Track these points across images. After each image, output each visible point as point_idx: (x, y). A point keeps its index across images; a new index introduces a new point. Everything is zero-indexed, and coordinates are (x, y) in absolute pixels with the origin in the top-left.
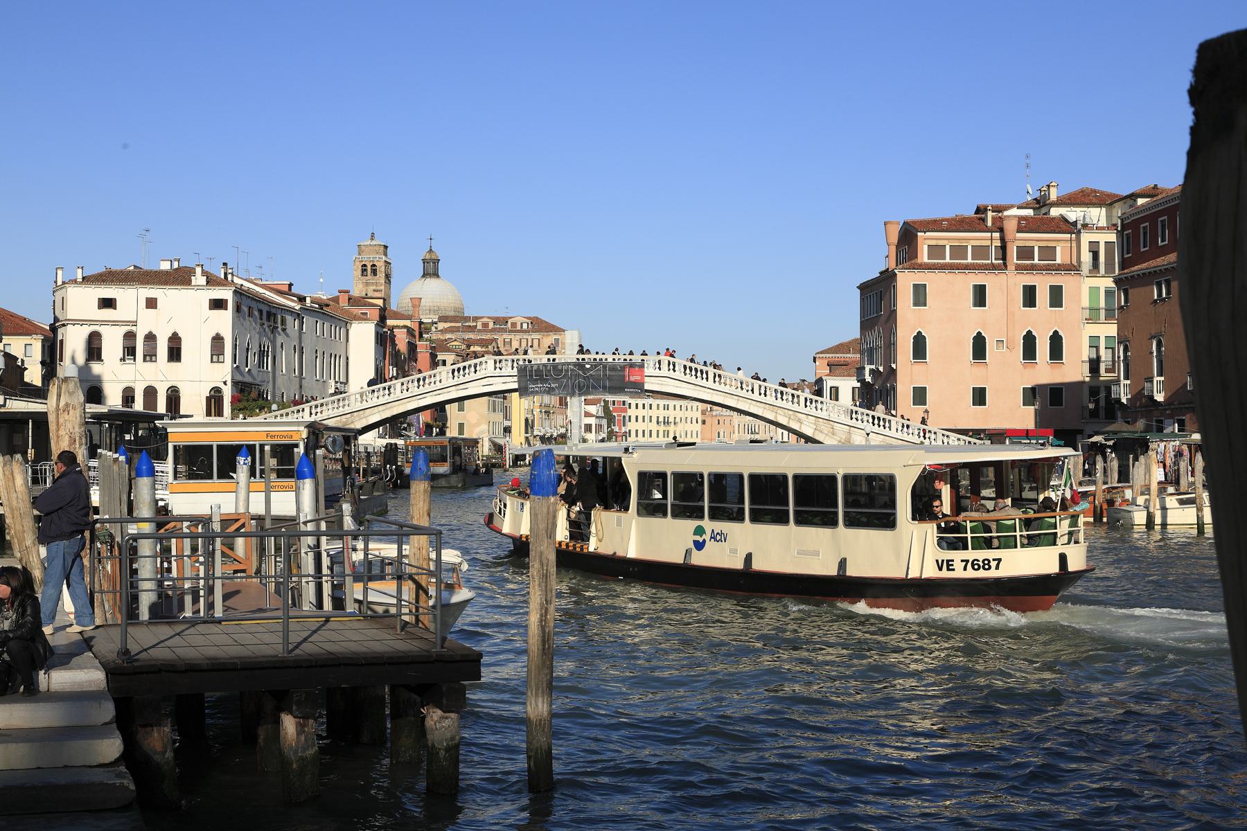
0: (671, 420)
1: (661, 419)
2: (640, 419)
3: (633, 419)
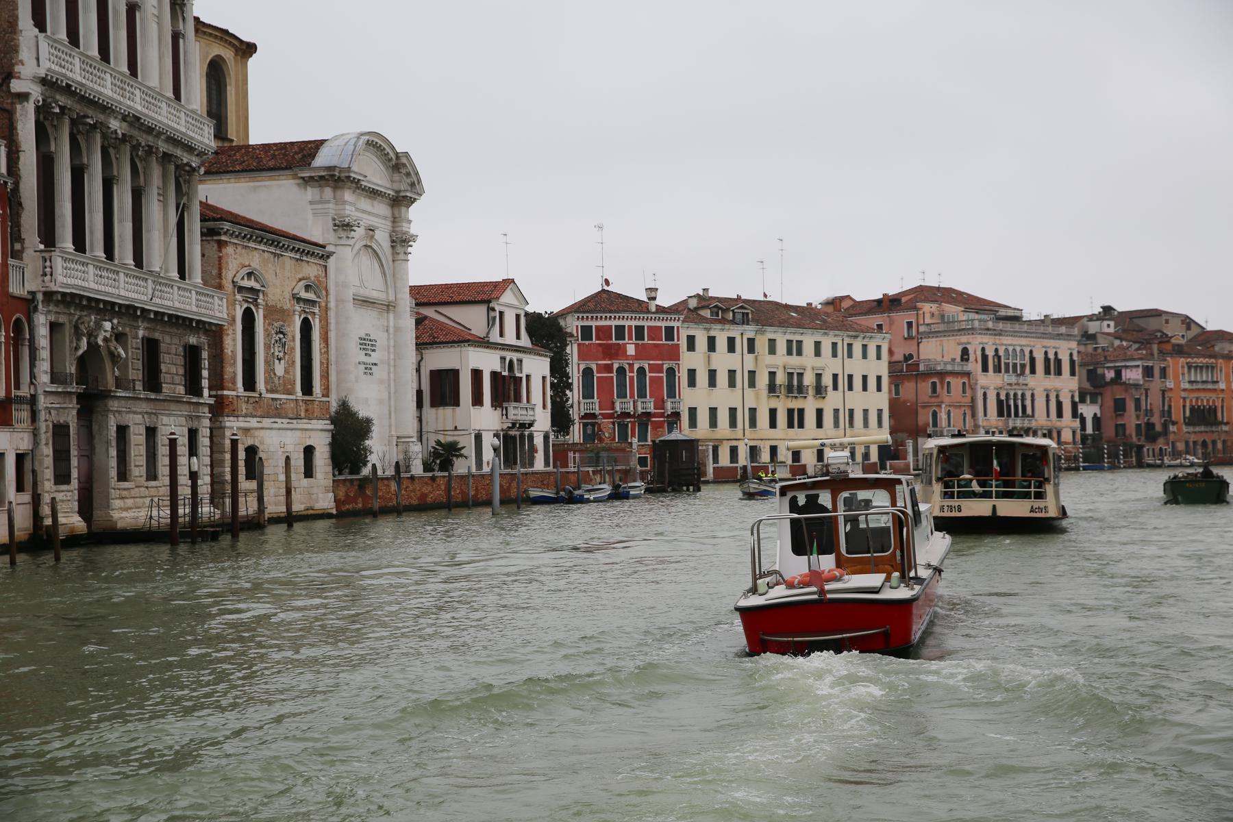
0: (809, 380)
1: (781, 379)
2: (722, 379)
3: (702, 378)
